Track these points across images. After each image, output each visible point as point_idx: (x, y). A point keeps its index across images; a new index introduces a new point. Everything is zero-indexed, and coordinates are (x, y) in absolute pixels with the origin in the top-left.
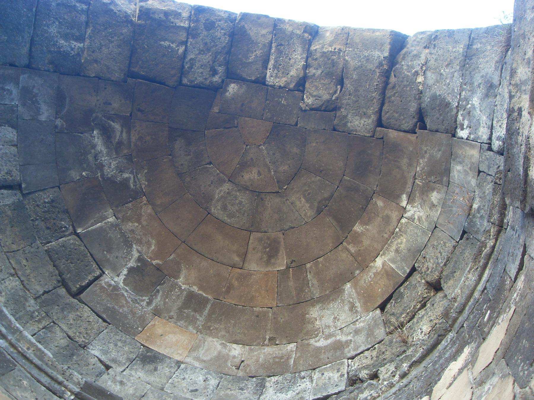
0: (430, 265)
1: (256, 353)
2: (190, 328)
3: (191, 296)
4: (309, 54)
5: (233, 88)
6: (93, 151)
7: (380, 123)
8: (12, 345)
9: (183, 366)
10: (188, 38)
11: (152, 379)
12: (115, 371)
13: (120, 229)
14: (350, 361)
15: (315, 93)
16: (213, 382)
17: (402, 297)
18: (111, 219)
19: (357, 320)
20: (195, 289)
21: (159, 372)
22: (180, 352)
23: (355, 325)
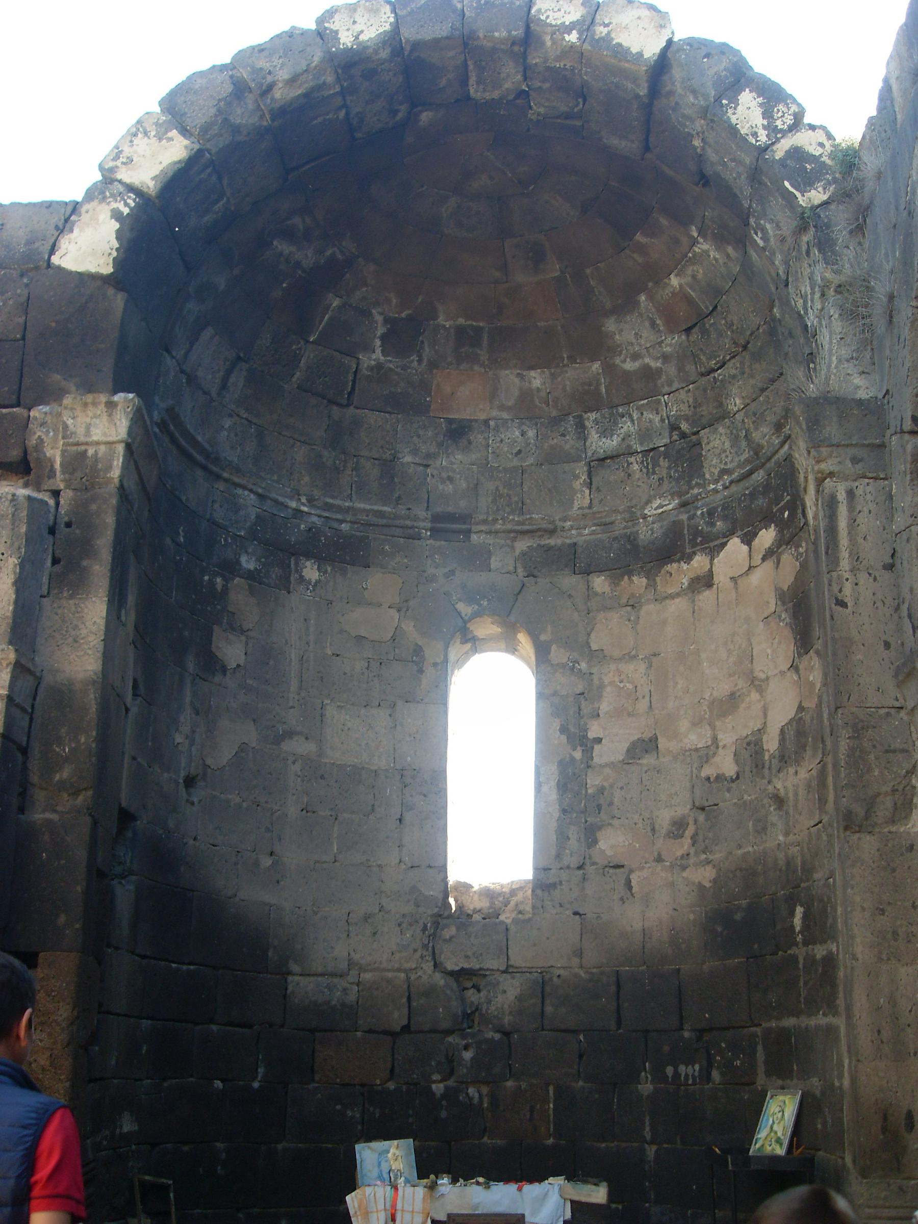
0: (735, 322)
1: (559, 379)
2: (476, 368)
3: (460, 331)
4: (527, 71)
5: (426, 117)
6: (282, 259)
7: (647, 148)
8: (351, 522)
9: (492, 423)
10: (345, 101)
11: (474, 457)
12: (435, 468)
13: (350, 306)
14: (666, 397)
15: (546, 104)
16: (531, 433)
17: (709, 336)
18: (336, 303)
19: (662, 342)
20: (461, 321)
21: (474, 444)
22: (481, 407)
23: (660, 346)
